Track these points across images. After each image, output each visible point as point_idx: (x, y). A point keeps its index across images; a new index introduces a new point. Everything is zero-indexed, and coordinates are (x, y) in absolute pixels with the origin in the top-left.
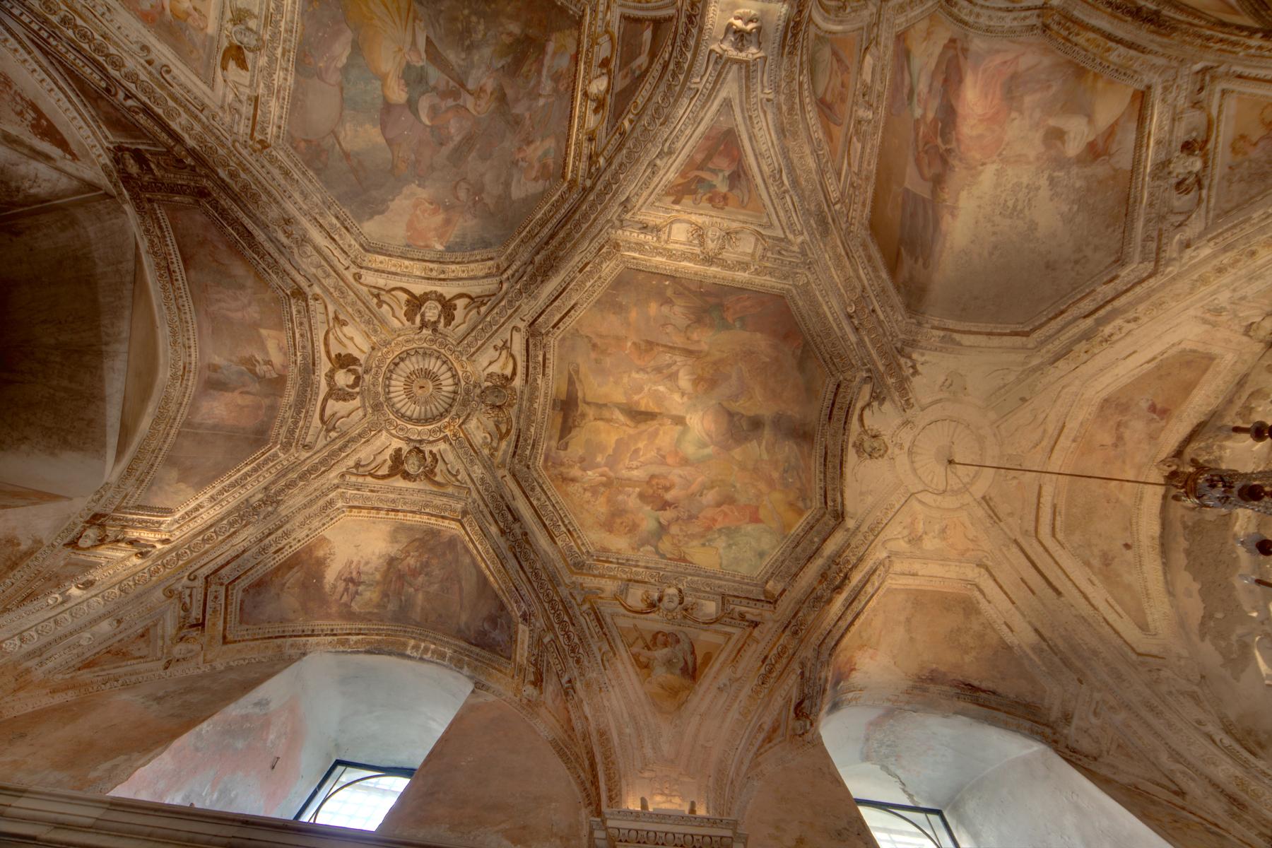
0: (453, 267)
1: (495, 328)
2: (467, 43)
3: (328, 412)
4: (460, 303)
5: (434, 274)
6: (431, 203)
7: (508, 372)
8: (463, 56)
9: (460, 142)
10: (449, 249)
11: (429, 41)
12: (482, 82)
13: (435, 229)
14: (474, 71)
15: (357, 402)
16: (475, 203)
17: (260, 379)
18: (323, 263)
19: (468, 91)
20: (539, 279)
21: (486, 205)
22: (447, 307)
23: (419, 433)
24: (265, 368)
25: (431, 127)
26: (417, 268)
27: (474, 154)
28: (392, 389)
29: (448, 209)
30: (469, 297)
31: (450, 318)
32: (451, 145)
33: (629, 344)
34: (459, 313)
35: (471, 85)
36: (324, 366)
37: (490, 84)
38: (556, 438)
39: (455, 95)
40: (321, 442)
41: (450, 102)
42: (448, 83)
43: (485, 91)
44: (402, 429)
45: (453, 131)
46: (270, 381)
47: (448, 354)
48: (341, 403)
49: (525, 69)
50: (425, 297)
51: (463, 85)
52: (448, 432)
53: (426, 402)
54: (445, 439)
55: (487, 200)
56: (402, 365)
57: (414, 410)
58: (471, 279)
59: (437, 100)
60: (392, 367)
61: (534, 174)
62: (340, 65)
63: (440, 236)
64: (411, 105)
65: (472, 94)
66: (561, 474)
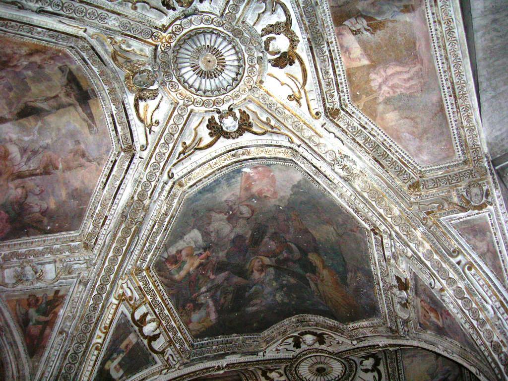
0: (226, 163)
1: (162, 141)
3: (280, 11)
4: (207, 140)
5: (240, 151)
6: (266, 197)
7: (142, 104)
9: (263, 238)
10: (239, 171)
11: (308, 285)
12: (263, 274)
14: (272, 277)
15: (259, 29)
16: (231, 208)
17: (359, 15)
18: (315, 149)
19: (271, 266)
20: (136, 198)
22: (217, 131)
23: (191, 22)
24: (358, 26)
26: (254, 152)
27: (248, 236)
28: (233, 51)
30: (200, 149)
31: (212, 125)
32: (268, 235)
33: (60, 166)
34: (205, 134)
35: (271, 270)
36: (302, 49)
37: (256, 275)
38: (75, 73)
41: (281, 257)
44: (207, 21)
46: (348, 16)
47: (198, 98)
48: (274, 22)
50: (240, 131)
52: (166, 35)
53: (199, 51)
54: (164, 29)
55: (221, 215)
56: (234, 75)
57: (206, 41)
58: (204, 163)
60: (241, 71)
61: (184, 253)
63: (248, 177)
66: (44, 53)
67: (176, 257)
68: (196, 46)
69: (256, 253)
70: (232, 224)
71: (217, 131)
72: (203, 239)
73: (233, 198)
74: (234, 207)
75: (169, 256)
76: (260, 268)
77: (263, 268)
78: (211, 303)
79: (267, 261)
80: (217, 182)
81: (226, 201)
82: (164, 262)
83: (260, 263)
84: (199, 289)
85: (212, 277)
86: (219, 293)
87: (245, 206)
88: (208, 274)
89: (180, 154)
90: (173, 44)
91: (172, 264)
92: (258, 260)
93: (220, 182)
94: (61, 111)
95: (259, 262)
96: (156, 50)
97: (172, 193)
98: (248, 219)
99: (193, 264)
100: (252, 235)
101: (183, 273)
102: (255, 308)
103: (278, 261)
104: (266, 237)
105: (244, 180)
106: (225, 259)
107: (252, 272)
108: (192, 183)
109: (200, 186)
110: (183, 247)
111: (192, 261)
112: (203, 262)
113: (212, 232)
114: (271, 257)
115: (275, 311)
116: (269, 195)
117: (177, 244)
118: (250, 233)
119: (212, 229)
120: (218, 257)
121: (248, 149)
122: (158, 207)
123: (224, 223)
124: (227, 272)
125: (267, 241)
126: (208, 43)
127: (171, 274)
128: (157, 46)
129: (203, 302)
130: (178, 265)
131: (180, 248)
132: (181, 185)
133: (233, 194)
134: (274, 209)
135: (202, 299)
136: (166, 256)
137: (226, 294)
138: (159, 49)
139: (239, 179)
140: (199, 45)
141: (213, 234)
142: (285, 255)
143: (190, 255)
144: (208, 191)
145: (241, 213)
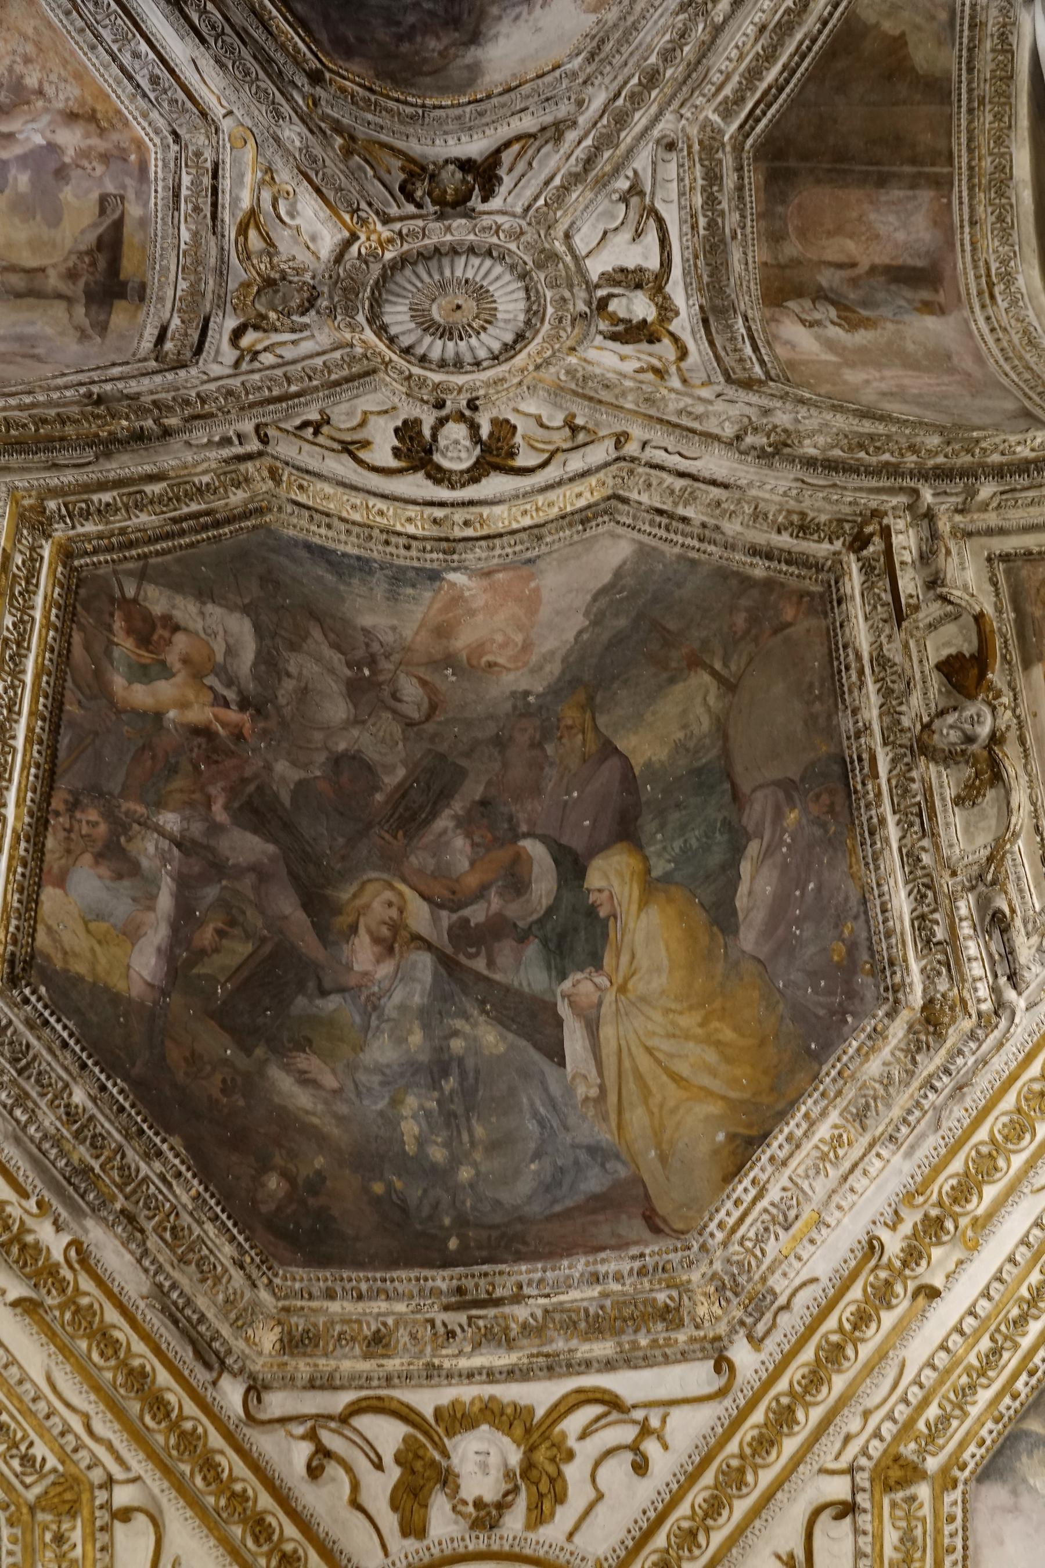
2: (450, 1084)
3: (652, 237)
6: (490, 665)
8: (457, 1045)
9: (434, 815)
12: (385, 969)
13: (472, 613)
15: (596, 268)
16: (372, 661)
17: (821, 296)
18: (695, 425)
19: (429, 946)
21: (336, 647)
22: (416, 451)
24: (817, 316)
25: (517, 837)
29: (449, 660)
31: (408, 431)
32: (458, 806)
35: (424, 961)
36: (684, 324)
37: (362, 954)
38: (128, 229)
39: (465, 935)
40: (642, 162)
41: (477, 914)
42: (491, 964)
43: (376, 940)
45: (460, 842)
46: (799, 293)
48: (631, 265)
49: (241, 949)
50: (475, 474)
51: (447, 963)
55: (337, 659)
57: (465, 269)
59: (513, 910)
61: (180, 640)
62: (753, 848)
63: (457, 599)
64: (572, 866)
65: (416, 938)
66: (102, 132)
67: (154, 628)
68: (442, 274)
69: (392, 862)
70: (355, 706)
71: (416, 451)
72: (255, 665)
73: (389, 638)
74: (385, 665)
75: (135, 601)
76: (385, 931)
77: (394, 940)
78: (165, 901)
79: (419, 915)
80: (363, 566)
81: (365, 631)
82: (112, 600)
83: (394, 913)
84: (160, 804)
85: (219, 814)
86: (211, 893)
87: (414, 681)
88: (213, 790)
89: (305, 424)
90: (388, 256)
91: (130, 632)
92: (388, 895)
93: (371, 572)
94: (31, 300)
95: (390, 904)
96: (347, 244)
97: (242, 467)
98: (410, 724)
99: (184, 705)
100: (403, 791)
101: (141, 695)
102: (302, 1099)
103: (465, 935)
104: (448, 812)
105: (437, 605)
106: (286, 798)
107: (354, 929)
108: (302, 498)
109: (320, 535)
110: (191, 625)
111: (191, 695)
112: (216, 734)
113: (289, 675)
114: (441, 906)
115: (378, 1188)
116: (501, 661)
117: (179, 600)
118: (401, 772)
119: (293, 669)
120: (268, 768)
121: (486, 511)
122: (194, 457)
123: (334, 687)
124: (271, 848)
125: (445, 831)
126: (470, 274)
127: (108, 653)
128: (354, 237)
129: (145, 863)
130: (146, 657)
131: (178, 615)
132: (274, 475)
133: (394, 629)
134: (508, 706)
135: (147, 848)
136: (130, 592)
137: (232, 923)
138: (354, 249)
139: (428, 595)
140: (447, 273)
141: (289, 685)
142: (495, 902)
143: (197, 670)
144: (329, 562)
145: (395, 696)
